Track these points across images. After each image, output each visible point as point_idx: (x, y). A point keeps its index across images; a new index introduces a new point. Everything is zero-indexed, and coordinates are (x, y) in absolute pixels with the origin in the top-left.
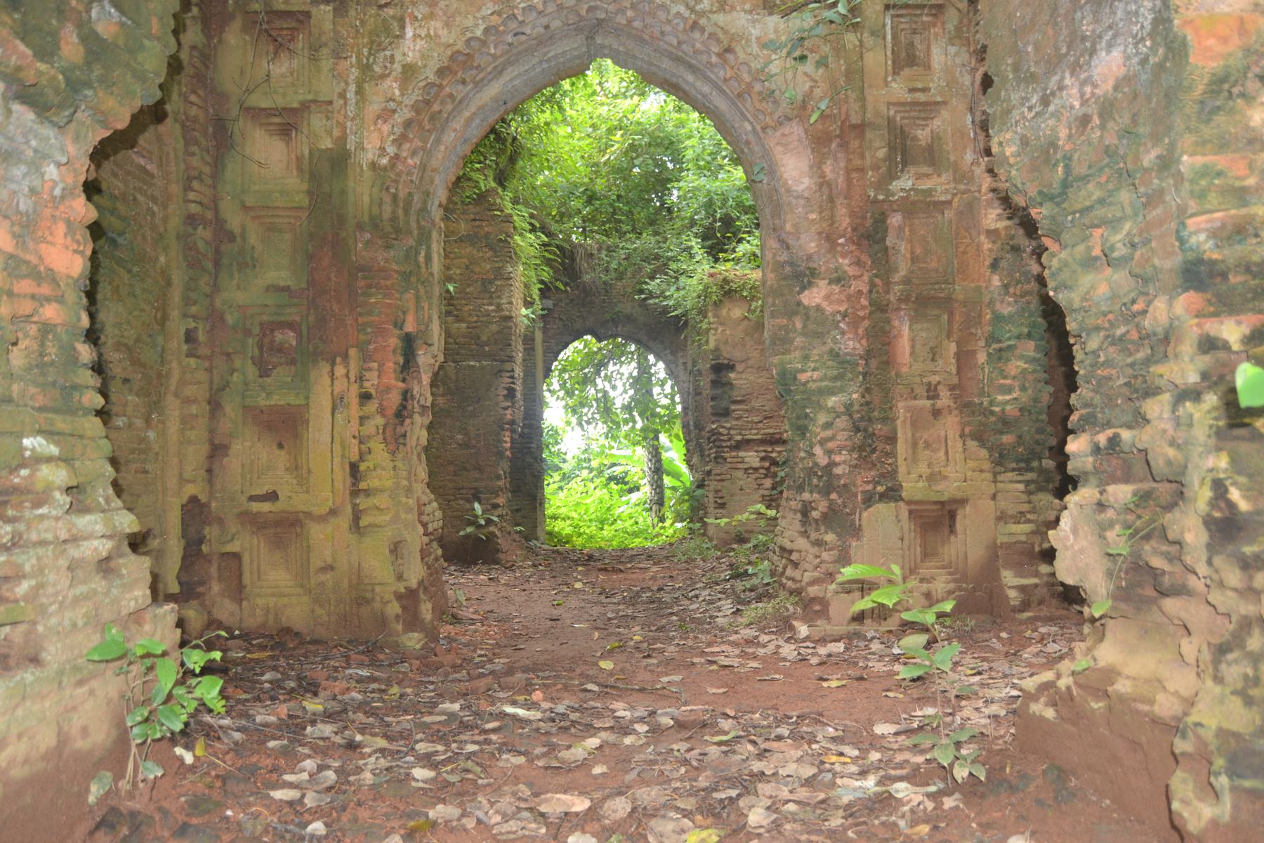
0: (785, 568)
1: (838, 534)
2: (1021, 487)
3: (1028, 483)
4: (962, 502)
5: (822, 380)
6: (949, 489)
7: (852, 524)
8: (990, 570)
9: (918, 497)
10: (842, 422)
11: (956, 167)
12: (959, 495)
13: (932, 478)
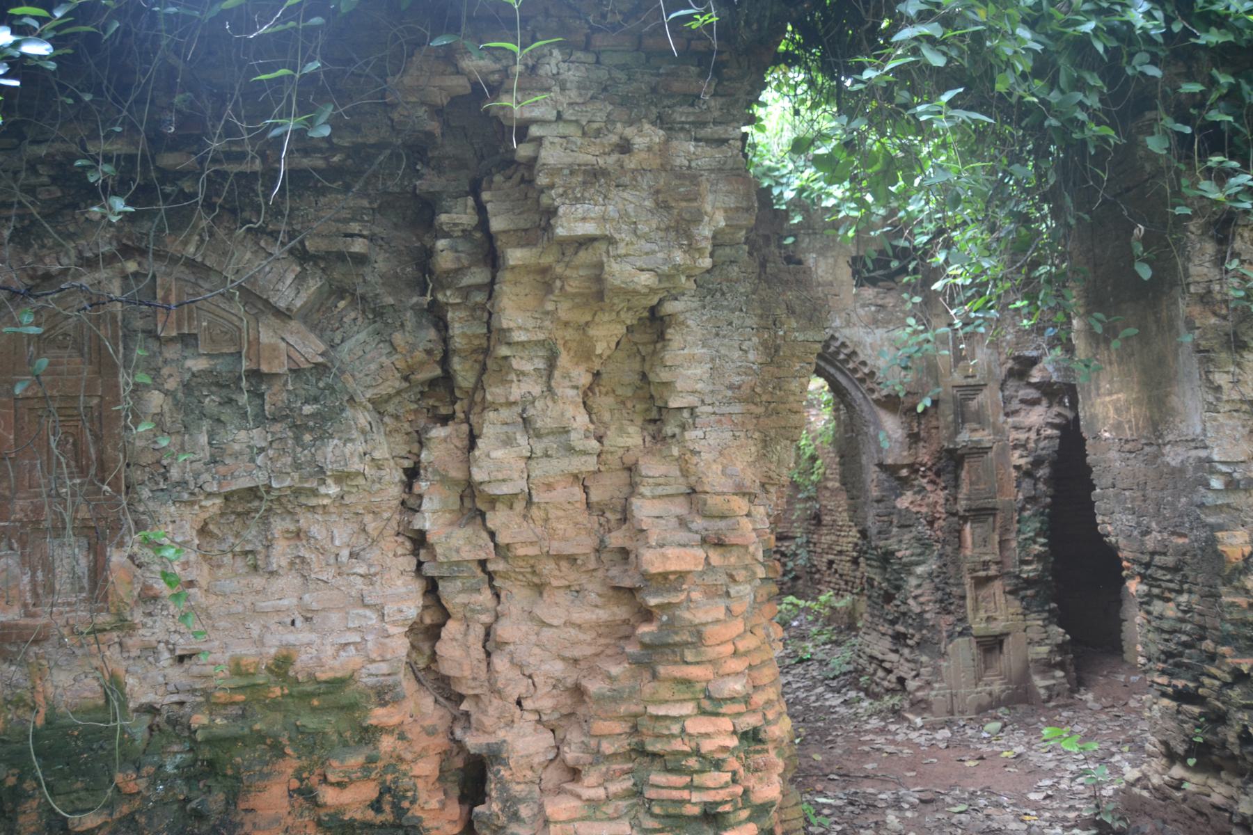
0: (875, 671)
1: (932, 658)
2: (1040, 623)
3: (1044, 620)
4: (1007, 634)
5: (912, 555)
6: (997, 627)
7: (939, 651)
8: (1025, 677)
9: (982, 633)
10: (927, 586)
11: (994, 426)
12: (1005, 631)
13: (989, 619)
